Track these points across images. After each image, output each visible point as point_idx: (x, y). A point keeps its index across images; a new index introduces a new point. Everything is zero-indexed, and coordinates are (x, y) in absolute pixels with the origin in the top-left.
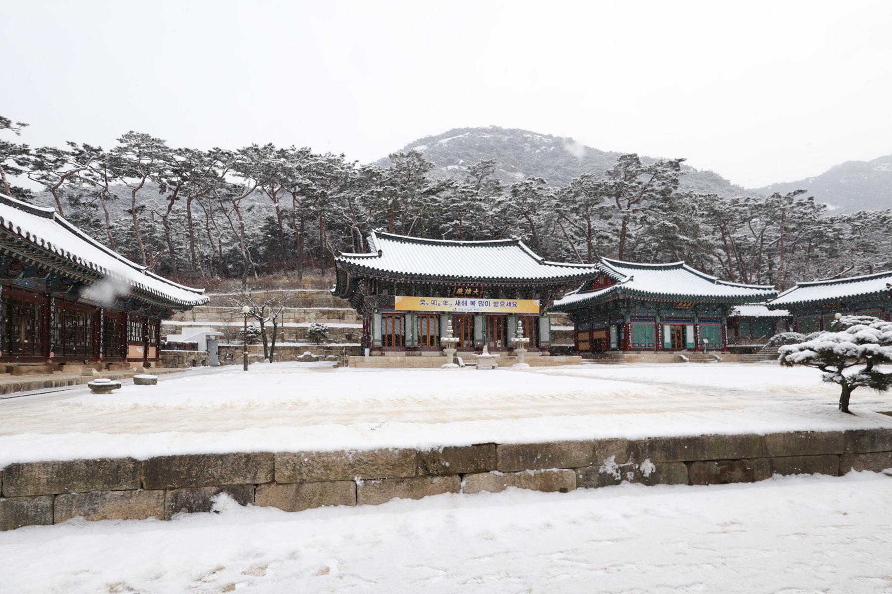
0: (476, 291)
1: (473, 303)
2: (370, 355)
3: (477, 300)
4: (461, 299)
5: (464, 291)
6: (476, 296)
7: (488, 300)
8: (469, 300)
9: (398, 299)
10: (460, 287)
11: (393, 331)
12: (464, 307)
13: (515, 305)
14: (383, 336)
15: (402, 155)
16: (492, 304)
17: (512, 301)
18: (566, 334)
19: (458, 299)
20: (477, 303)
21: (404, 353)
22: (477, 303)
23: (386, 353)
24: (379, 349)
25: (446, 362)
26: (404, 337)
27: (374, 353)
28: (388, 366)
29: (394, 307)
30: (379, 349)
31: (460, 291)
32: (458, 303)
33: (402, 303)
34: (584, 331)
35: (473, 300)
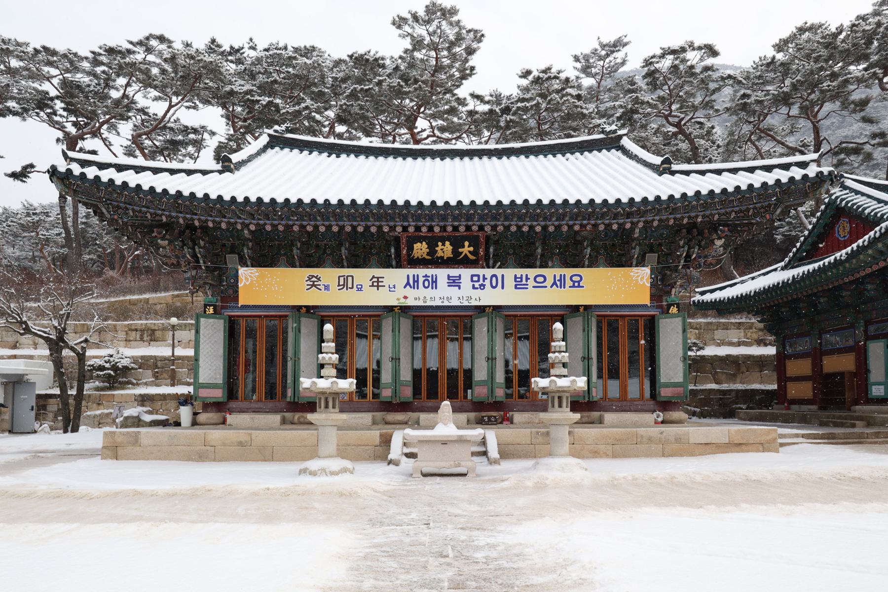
0: (466, 249)
1: (454, 282)
2: (194, 423)
3: (465, 273)
4: (421, 272)
5: (432, 251)
6: (466, 263)
7: (498, 272)
8: (442, 274)
9: (247, 275)
10: (420, 239)
11: (461, 362)
12: (429, 293)
13: (577, 285)
14: (416, 373)
15: (415, 17)
16: (510, 282)
17: (568, 272)
18: (760, 362)
19: (412, 272)
20: (466, 281)
21: (277, 418)
22: (466, 281)
23: (230, 418)
24: (218, 406)
25: (314, 454)
26: (469, 374)
27: (202, 417)
28: (201, 457)
29: (236, 299)
30: (218, 406)
31: (421, 249)
32: (412, 283)
33: (263, 287)
34: (798, 356)
35: (454, 272)
